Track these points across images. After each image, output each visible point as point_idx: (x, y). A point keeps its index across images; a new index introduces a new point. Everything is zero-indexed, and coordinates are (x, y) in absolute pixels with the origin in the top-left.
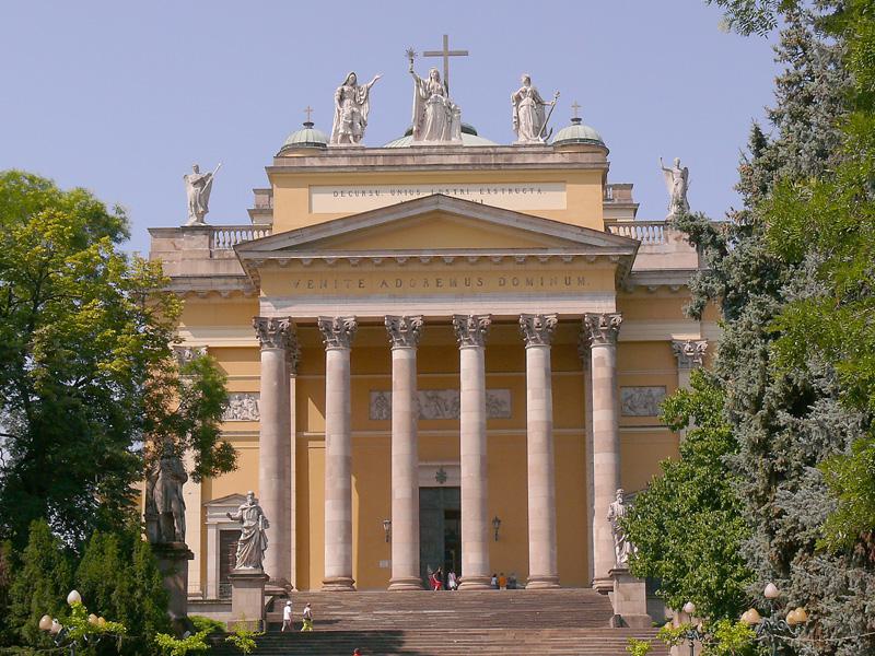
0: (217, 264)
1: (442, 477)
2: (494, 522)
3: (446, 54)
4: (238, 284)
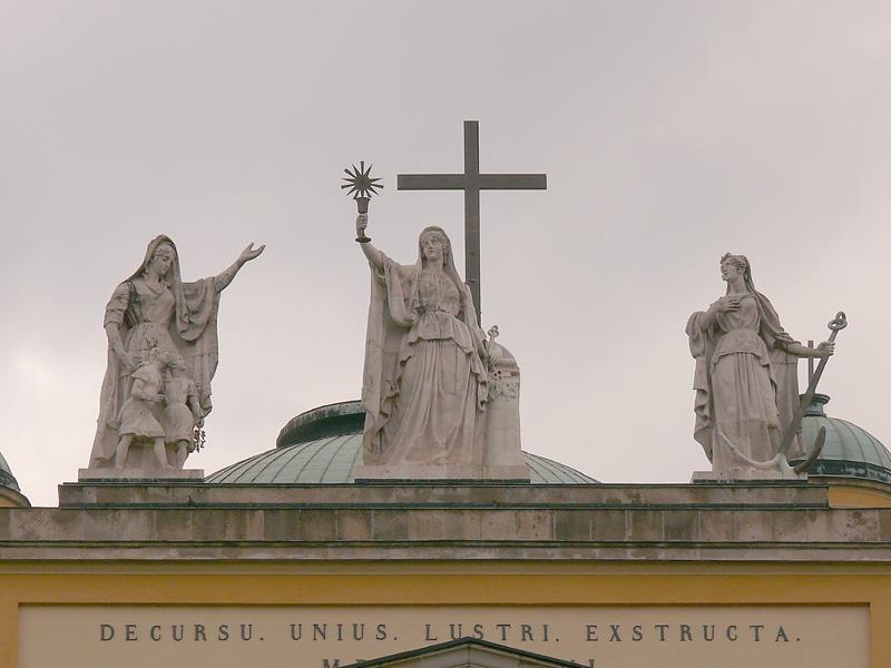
3: (472, 182)
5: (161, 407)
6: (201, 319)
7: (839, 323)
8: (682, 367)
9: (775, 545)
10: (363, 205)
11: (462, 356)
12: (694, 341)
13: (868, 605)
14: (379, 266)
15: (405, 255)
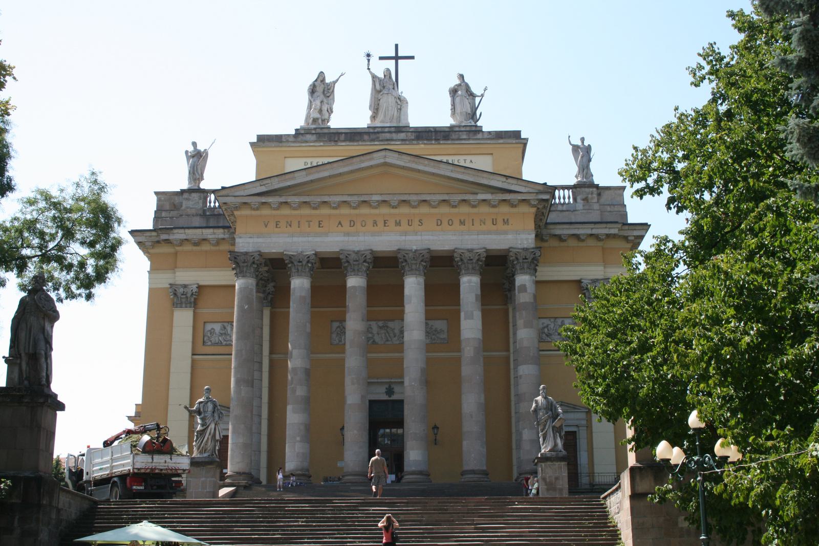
0: (208, 220)
1: (390, 392)
2: (433, 428)
3: (397, 58)
4: (224, 234)
5: (320, 111)
6: (331, 90)
7: (485, 90)
8: (448, 99)
9: (469, 139)
10: (369, 60)
11: (393, 98)
12: (450, 94)
13: (492, 154)
14: (374, 77)
15: (381, 75)
